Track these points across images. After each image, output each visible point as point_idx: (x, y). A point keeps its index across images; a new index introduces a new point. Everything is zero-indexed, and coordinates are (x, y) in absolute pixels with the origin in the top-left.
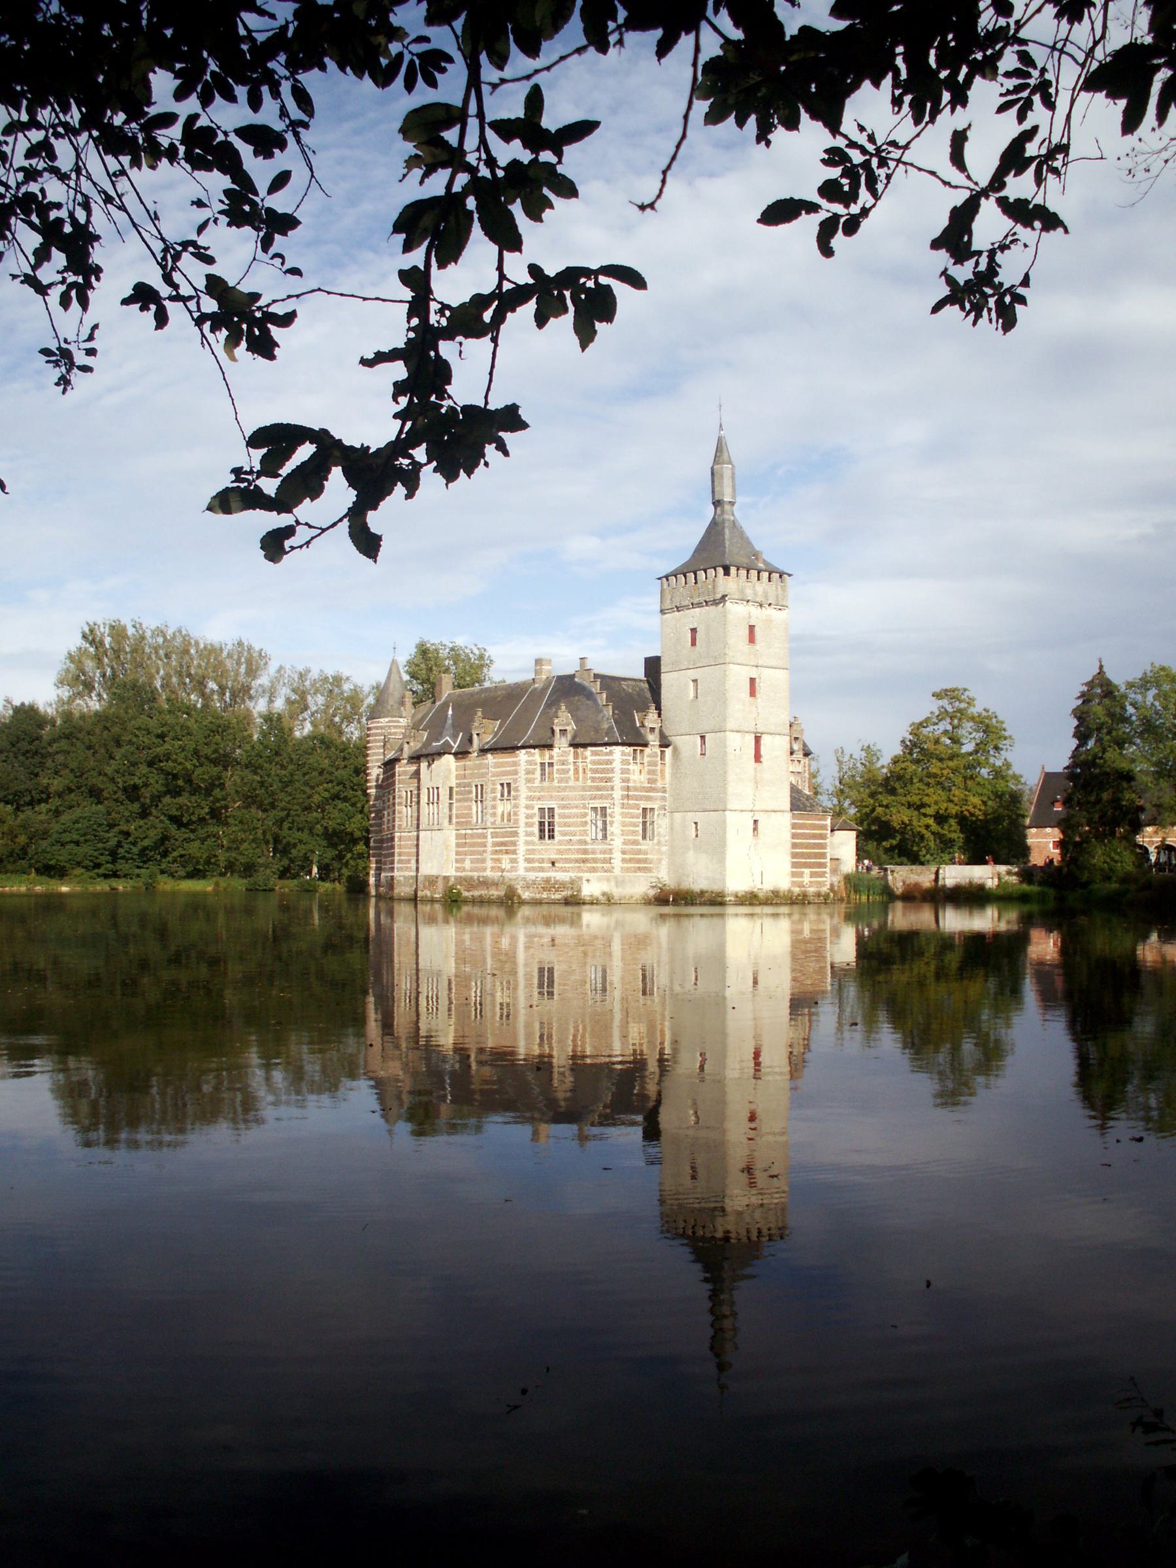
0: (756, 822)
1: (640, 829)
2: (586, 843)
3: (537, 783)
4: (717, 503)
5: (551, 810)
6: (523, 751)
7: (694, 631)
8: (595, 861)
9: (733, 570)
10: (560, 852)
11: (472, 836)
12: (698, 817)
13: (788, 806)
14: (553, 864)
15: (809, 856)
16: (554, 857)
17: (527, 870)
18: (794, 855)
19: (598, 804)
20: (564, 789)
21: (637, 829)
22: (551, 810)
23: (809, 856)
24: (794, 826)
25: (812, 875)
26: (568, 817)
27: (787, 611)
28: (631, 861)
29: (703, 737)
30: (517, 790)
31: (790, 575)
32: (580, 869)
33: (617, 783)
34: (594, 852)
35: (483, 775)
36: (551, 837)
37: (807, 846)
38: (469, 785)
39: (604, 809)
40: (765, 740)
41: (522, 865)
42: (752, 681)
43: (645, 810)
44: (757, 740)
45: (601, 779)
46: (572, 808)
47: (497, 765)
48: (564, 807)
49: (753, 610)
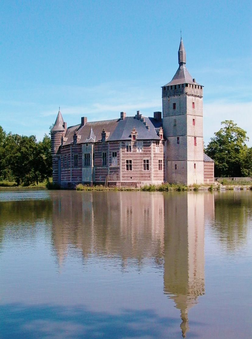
0: (195, 164)
1: (158, 167)
2: (142, 171)
3: (126, 152)
4: (181, 64)
5: (131, 161)
6: (121, 142)
7: (174, 104)
8: (146, 177)
9: (189, 85)
10: (133, 174)
11: (101, 169)
12: (178, 163)
14: (131, 178)
16: (131, 175)
17: (123, 180)
18: (205, 175)
19: (146, 159)
20: (135, 154)
21: (157, 167)
22: (131, 161)
26: (136, 163)
27: (202, 98)
28: (156, 176)
29: (178, 138)
30: (119, 154)
31: (203, 87)
32: (140, 180)
33: (152, 152)
34: (145, 174)
35: (107, 150)
36: (131, 169)
38: (101, 153)
39: (148, 161)
40: (197, 138)
41: (121, 178)
42: (194, 120)
43: (159, 161)
44: (195, 138)
45: (147, 151)
46: (137, 160)
47: (111, 146)
48: (135, 160)
49: (194, 98)
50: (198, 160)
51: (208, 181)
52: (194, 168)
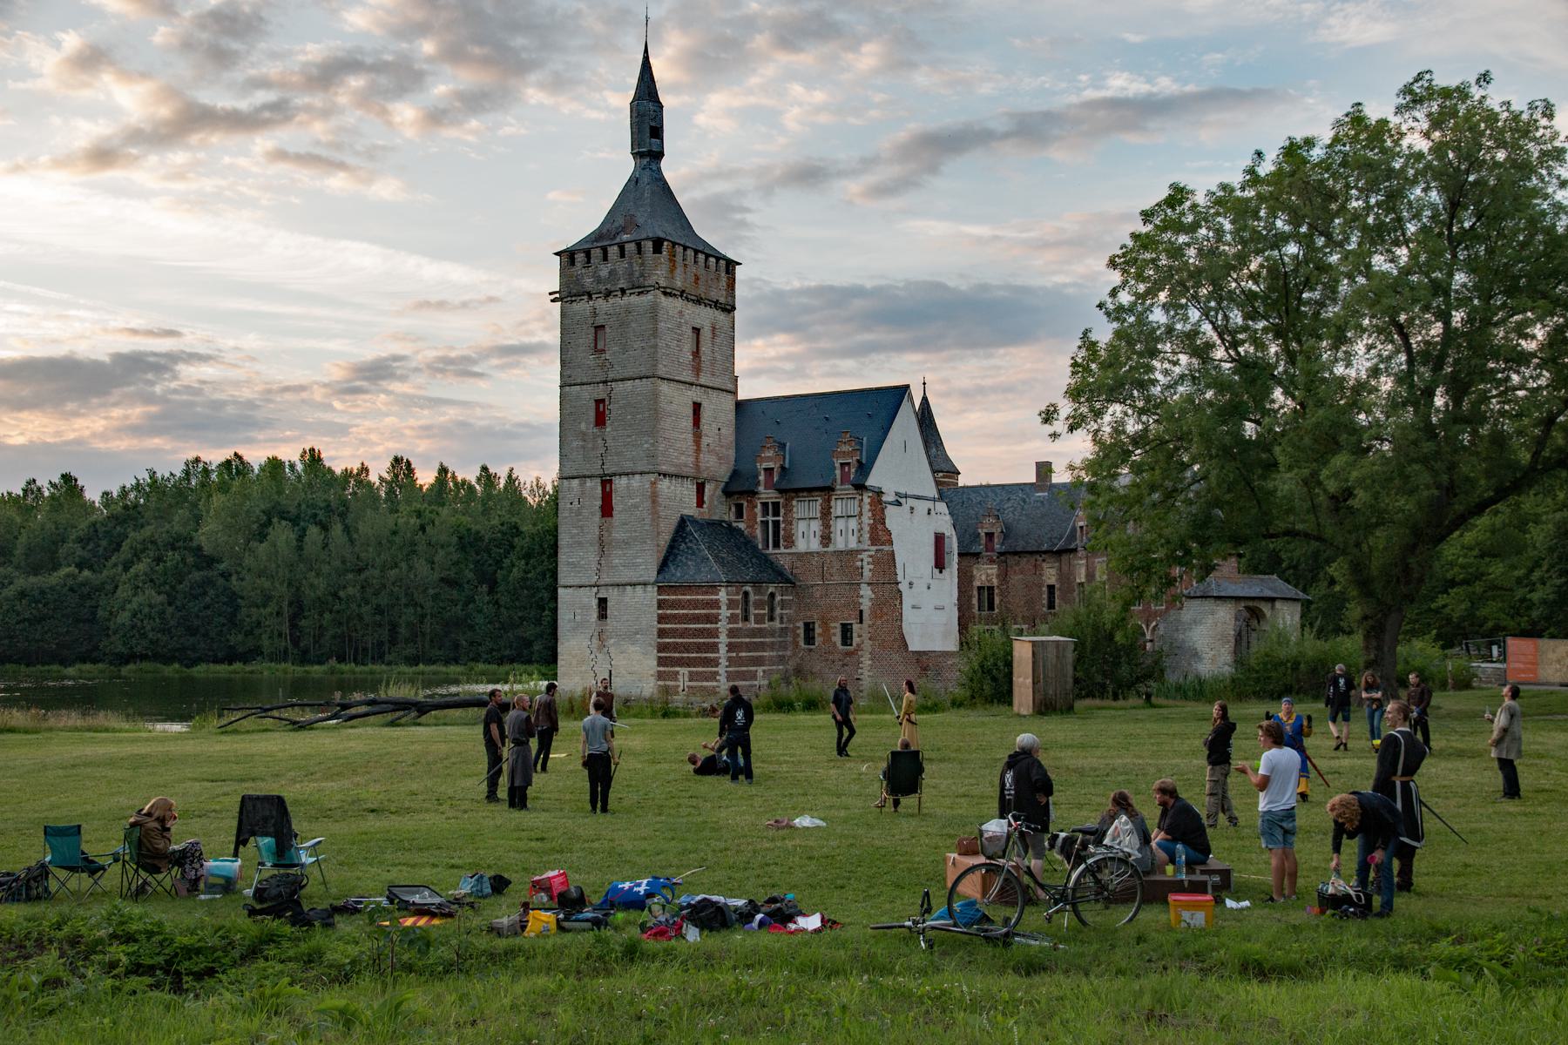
0: (603, 602)
15: (687, 648)
23: (687, 648)
24: (661, 604)
25: (692, 677)
37: (683, 634)
40: (620, 483)
44: (606, 482)
49: (601, 304)
50: (625, 580)
51: (680, 677)
52: (595, 615)
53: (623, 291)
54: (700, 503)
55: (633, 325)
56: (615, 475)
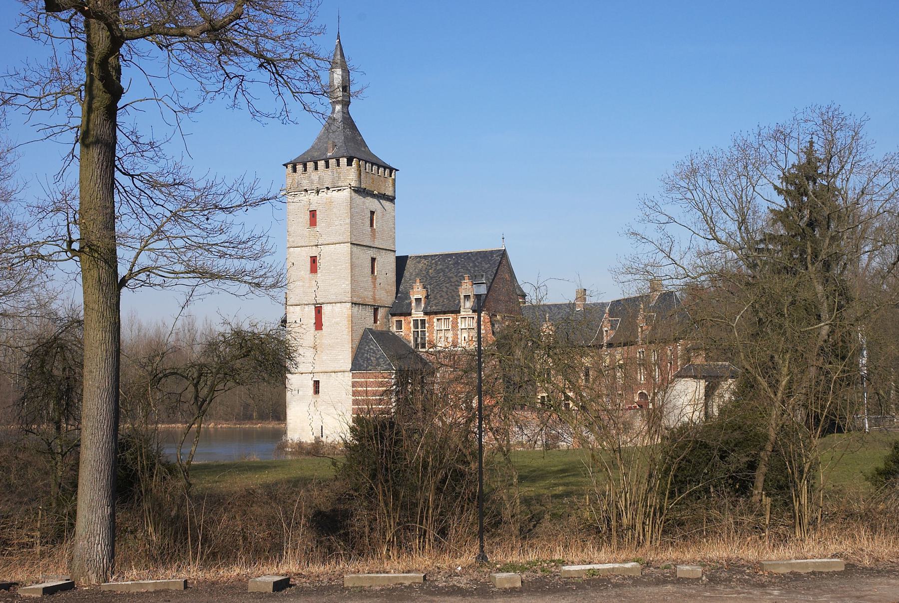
0: (317, 383)
13: (349, 366)
24: (354, 385)
40: (326, 309)
42: (314, 260)
44: (318, 311)
49: (313, 197)
53: (328, 188)
54: (375, 322)
55: (335, 210)
56: (323, 303)
